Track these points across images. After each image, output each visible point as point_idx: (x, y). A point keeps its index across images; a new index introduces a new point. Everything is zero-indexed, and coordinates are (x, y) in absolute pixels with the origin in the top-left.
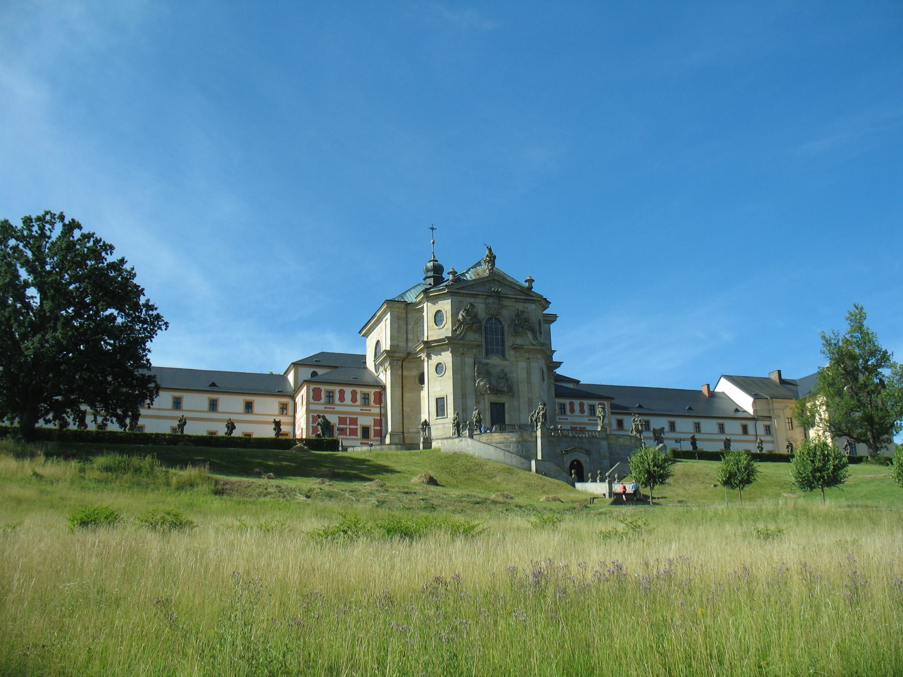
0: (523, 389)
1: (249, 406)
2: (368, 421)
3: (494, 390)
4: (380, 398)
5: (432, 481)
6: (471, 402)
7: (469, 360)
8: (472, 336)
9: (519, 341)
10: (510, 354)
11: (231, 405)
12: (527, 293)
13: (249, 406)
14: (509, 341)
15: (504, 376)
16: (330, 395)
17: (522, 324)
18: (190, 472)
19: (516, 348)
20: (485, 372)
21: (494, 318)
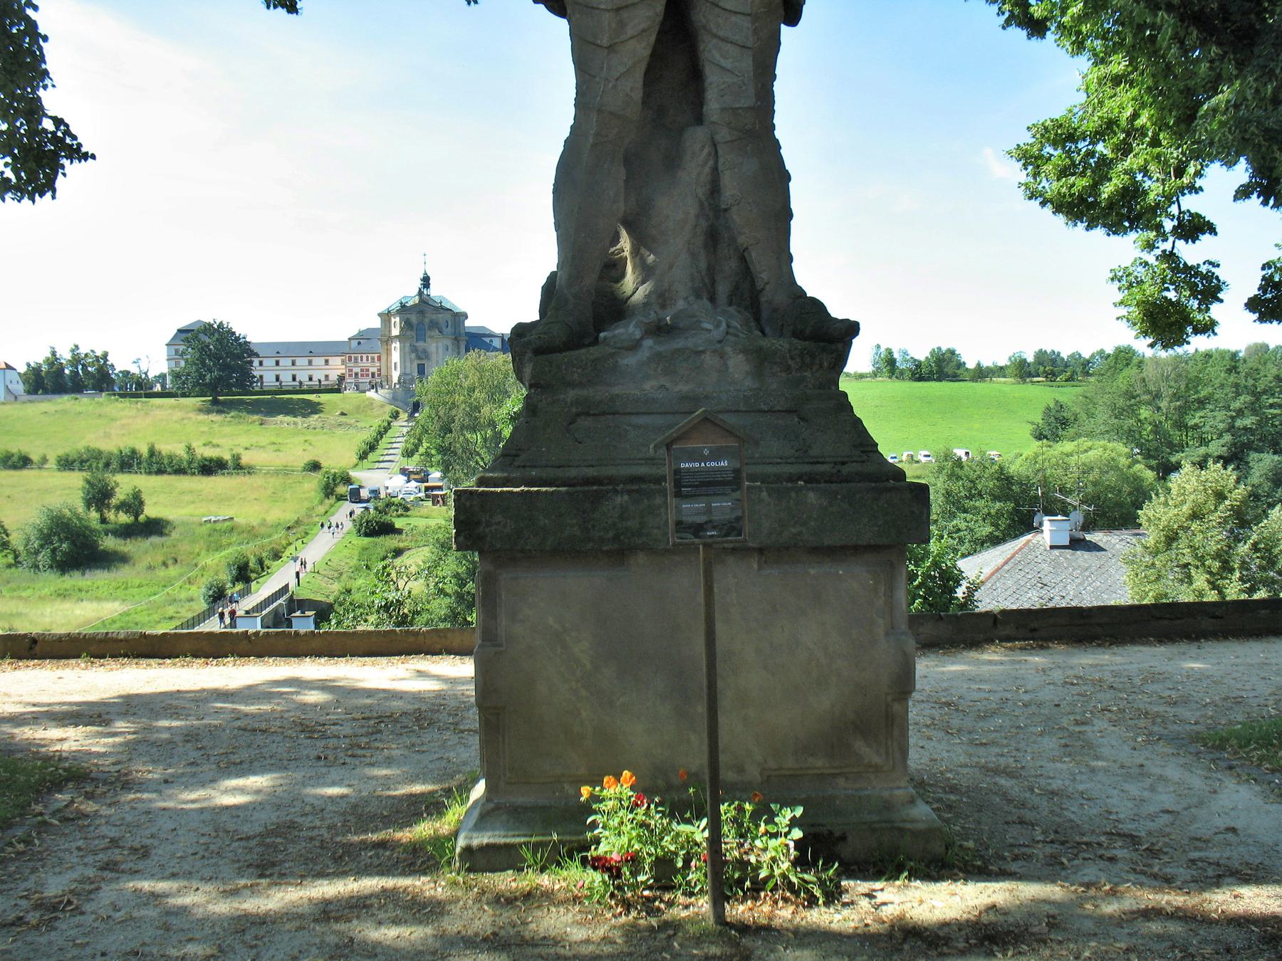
0: (434, 356)
1: (327, 361)
2: (374, 370)
3: (419, 358)
4: (379, 358)
5: (343, 414)
6: (408, 364)
7: (408, 344)
8: (409, 333)
10: (429, 340)
11: (318, 361)
13: (327, 361)
14: (428, 333)
15: (425, 352)
16: (356, 359)
17: (434, 325)
18: (256, 417)
20: (414, 349)
21: (421, 323)
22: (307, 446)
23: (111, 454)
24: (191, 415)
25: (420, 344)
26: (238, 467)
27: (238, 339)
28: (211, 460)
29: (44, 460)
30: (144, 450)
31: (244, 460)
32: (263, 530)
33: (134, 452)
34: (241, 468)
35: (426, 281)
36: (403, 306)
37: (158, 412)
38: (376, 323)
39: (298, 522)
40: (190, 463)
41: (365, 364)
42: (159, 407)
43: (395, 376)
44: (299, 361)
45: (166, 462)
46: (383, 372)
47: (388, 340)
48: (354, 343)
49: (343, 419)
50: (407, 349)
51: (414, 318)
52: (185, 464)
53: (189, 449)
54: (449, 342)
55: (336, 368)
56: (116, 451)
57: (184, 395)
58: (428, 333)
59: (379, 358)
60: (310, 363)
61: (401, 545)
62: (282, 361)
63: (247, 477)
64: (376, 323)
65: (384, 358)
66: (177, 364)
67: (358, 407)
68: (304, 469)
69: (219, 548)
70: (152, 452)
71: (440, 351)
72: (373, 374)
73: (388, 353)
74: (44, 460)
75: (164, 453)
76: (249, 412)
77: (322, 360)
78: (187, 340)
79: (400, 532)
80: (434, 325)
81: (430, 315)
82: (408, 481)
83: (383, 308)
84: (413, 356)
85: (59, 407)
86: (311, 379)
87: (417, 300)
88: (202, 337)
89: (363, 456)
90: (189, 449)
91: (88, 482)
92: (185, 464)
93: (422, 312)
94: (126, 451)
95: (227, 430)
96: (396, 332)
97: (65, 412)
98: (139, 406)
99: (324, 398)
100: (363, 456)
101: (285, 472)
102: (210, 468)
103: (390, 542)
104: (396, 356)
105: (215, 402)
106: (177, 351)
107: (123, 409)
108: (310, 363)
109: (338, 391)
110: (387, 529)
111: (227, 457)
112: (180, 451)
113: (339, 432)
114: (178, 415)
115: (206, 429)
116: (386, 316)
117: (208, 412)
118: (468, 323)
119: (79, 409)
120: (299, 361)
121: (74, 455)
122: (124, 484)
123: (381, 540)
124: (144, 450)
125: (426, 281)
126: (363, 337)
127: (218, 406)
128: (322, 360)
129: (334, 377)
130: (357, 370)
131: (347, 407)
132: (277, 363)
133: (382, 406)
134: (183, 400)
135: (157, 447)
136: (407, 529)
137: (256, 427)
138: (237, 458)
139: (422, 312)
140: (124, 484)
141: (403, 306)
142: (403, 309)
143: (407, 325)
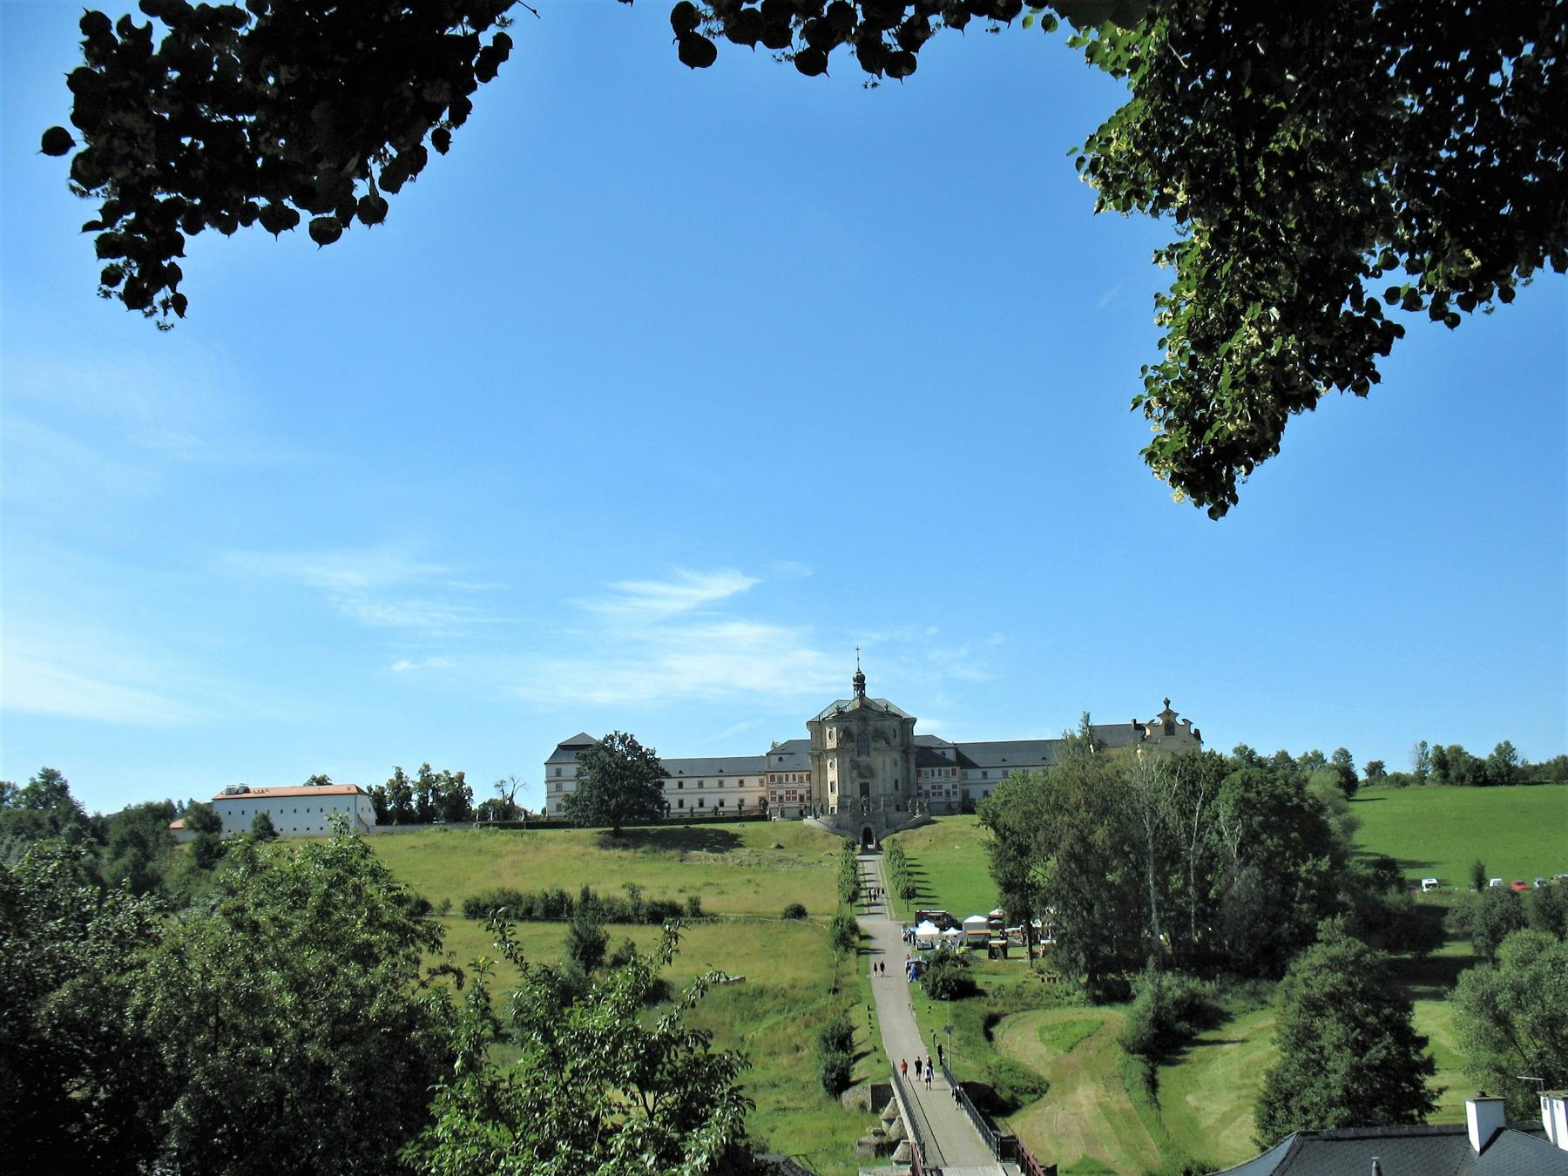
1: (741, 783)
2: (800, 792)
4: (809, 778)
5: (779, 847)
6: (848, 784)
7: (847, 760)
8: (848, 745)
9: (878, 745)
10: (873, 753)
12: (887, 714)
13: (741, 783)
14: (873, 745)
16: (780, 779)
17: (879, 734)
18: (673, 852)
19: (876, 750)
20: (855, 765)
22: (752, 888)
23: (532, 899)
24: (594, 850)
25: (863, 759)
26: (697, 913)
27: (644, 755)
28: (663, 905)
29: (447, 905)
30: (575, 894)
31: (707, 904)
32: (799, 993)
33: (562, 895)
34: (702, 915)
35: (860, 682)
36: (840, 712)
37: (550, 846)
38: (807, 735)
39: (836, 982)
40: (636, 909)
41: (791, 784)
42: (550, 840)
43: (833, 799)
44: (708, 783)
45: (605, 907)
46: (815, 795)
47: (819, 754)
48: (775, 759)
49: (780, 853)
50: (847, 765)
51: (854, 727)
52: (630, 911)
53: (634, 891)
54: (897, 755)
55: (753, 792)
56: (538, 894)
57: (580, 826)
58: (873, 745)
59: (809, 778)
60: (721, 784)
61: (995, 1010)
62: (687, 783)
63: (712, 927)
64: (807, 735)
65: (815, 777)
66: (559, 788)
67: (797, 838)
68: (785, 916)
69: (757, 1017)
70: (586, 895)
71: (888, 765)
72: (802, 798)
73: (822, 771)
74: (447, 905)
75: (601, 896)
76: (667, 847)
77: (734, 781)
78: (584, 758)
79: (982, 993)
80: (879, 734)
81: (874, 724)
82: (943, 929)
83: (812, 716)
84: (855, 773)
85: (428, 840)
86: (722, 804)
87: (857, 704)
88: (602, 754)
89: (853, 898)
90: (634, 891)
91: (576, 933)
92: (630, 911)
93: (864, 719)
94: (553, 895)
95: (642, 868)
96: (831, 744)
97: (436, 847)
98: (526, 838)
99: (751, 826)
100: (853, 898)
101: (752, 918)
102: (660, 914)
103: (976, 1009)
104: (832, 775)
105: (617, 834)
106: (558, 773)
107: (506, 843)
108: (721, 784)
109: (763, 818)
110: (963, 990)
111: (682, 900)
112: (623, 895)
113: (783, 868)
114: (577, 849)
115: (615, 867)
116: (817, 726)
117: (615, 846)
118: (919, 730)
119: (453, 843)
120: (708, 783)
121: (486, 900)
122: (616, 937)
123: (966, 1002)
124: (575, 894)
125: (860, 682)
126: (783, 753)
127: (619, 839)
128: (734, 781)
129: (752, 800)
130: (782, 792)
131: (783, 840)
132: (681, 785)
133: (826, 837)
134: (574, 831)
135: (592, 888)
136: (989, 990)
137: (676, 865)
138: (695, 903)
139: (864, 719)
140: (616, 937)
141: (840, 712)
142: (841, 715)
143: (846, 736)
